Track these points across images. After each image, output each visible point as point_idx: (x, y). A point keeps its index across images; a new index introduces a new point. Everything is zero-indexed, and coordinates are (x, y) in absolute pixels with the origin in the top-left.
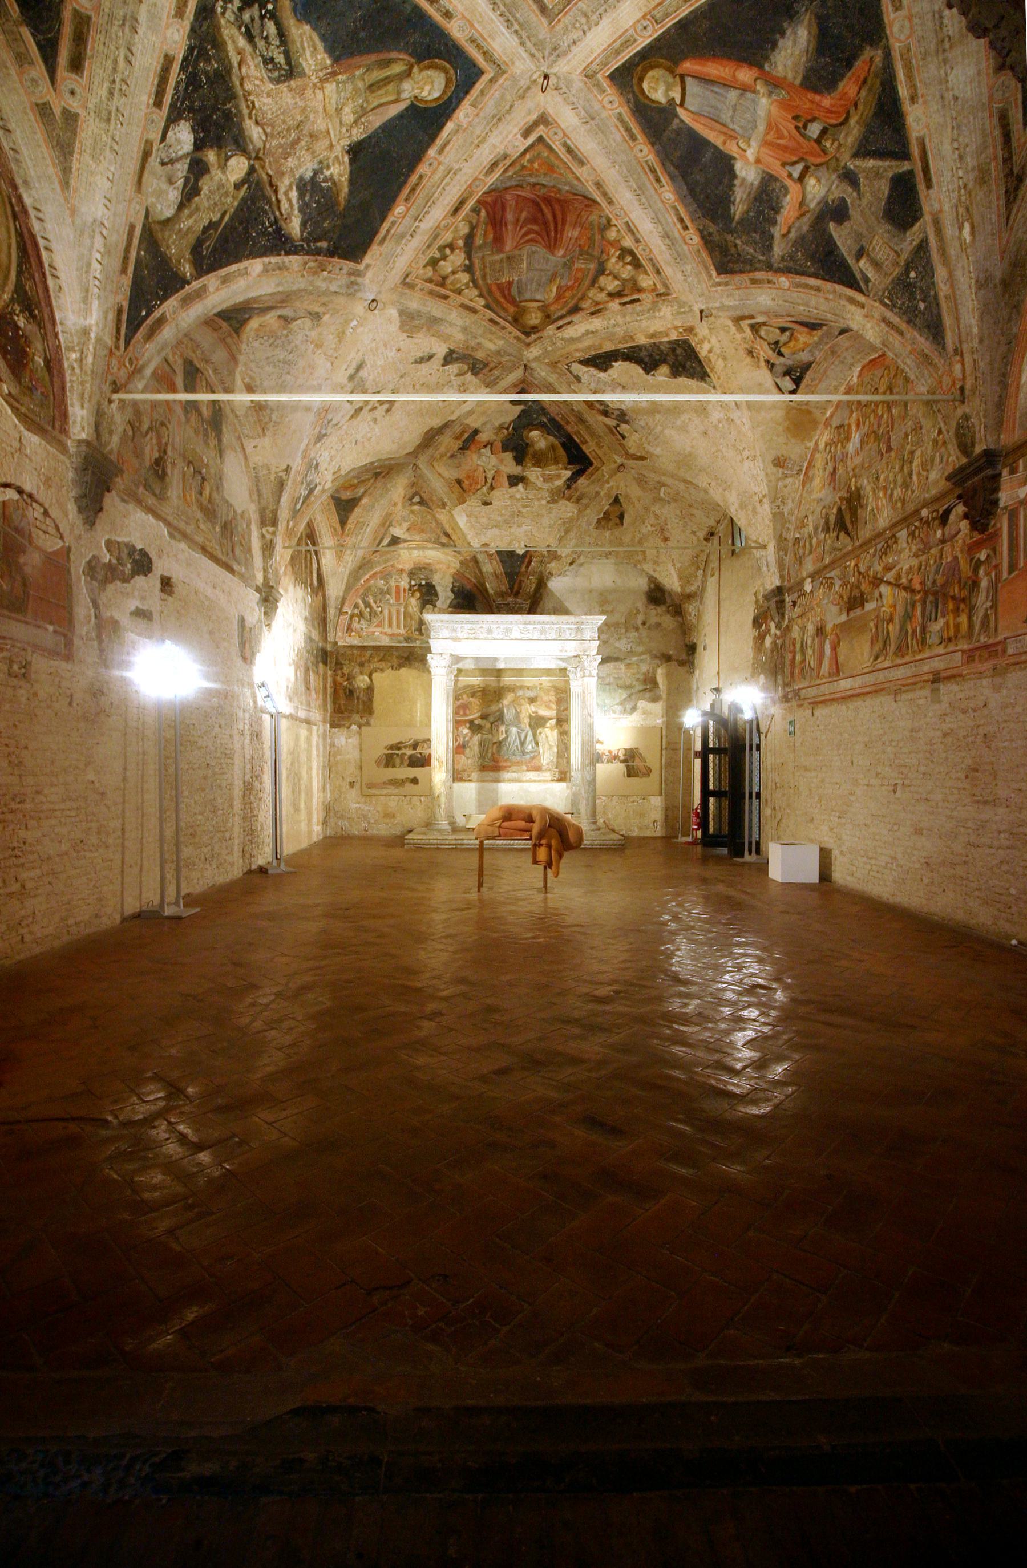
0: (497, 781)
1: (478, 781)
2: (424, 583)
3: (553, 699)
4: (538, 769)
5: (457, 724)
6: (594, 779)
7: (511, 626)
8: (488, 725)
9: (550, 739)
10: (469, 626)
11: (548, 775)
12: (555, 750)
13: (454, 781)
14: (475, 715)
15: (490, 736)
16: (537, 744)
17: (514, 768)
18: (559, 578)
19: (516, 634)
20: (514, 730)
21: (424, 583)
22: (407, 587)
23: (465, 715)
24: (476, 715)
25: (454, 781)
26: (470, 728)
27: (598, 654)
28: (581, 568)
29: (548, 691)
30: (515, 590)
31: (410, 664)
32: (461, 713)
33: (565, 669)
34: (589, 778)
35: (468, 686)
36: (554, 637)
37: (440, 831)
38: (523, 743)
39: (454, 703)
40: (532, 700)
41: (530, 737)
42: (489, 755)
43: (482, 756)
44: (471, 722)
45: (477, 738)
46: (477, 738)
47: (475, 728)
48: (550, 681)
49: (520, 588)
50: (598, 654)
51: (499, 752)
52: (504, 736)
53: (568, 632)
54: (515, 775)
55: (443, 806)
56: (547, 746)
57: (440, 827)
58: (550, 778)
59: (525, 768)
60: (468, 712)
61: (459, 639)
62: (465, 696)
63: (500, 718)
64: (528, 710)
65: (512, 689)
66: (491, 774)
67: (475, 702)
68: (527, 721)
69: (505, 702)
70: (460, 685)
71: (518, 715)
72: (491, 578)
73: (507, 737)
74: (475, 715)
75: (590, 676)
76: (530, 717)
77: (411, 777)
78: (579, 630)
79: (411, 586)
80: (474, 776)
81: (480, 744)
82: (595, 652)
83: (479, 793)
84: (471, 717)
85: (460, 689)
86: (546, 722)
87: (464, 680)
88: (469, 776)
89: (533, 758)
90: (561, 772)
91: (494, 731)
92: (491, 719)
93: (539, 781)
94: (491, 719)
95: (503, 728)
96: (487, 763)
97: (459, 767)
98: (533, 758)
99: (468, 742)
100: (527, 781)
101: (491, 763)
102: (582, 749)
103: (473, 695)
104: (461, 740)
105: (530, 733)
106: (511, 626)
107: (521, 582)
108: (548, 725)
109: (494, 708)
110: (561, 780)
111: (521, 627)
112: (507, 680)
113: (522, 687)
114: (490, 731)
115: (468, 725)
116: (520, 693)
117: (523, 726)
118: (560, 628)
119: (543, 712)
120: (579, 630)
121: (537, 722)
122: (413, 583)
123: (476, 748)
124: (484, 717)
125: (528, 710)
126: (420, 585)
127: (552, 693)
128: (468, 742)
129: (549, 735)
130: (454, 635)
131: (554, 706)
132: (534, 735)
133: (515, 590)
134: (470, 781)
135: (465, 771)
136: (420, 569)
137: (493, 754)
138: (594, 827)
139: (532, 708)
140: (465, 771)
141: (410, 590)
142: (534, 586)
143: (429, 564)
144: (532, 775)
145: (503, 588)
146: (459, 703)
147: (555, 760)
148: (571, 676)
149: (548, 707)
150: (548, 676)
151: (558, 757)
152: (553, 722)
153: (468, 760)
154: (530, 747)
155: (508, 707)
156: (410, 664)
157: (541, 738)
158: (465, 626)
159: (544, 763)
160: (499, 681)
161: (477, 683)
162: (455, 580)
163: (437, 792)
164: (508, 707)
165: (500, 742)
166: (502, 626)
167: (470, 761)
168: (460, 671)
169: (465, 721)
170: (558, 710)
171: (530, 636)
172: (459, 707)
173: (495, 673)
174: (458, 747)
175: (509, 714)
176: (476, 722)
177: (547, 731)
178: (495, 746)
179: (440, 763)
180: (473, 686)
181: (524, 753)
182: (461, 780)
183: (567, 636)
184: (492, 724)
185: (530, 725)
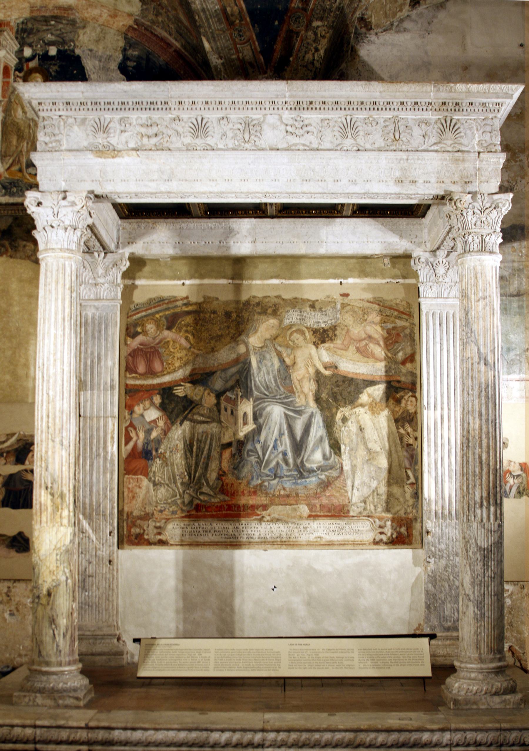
0: (234, 543)
1: (182, 544)
2: (53, 51)
3: (377, 331)
4: (339, 512)
5: (131, 396)
6: (499, 544)
7: (256, 115)
8: (210, 400)
9: (371, 434)
10: (144, 116)
11: (365, 530)
12: (383, 462)
13: (120, 544)
14: (174, 373)
15: (213, 428)
16: (336, 447)
17: (276, 510)
18: (387, 37)
19: (271, 135)
20: (276, 412)
21: (53, 51)
22: (13, 62)
23: (151, 373)
24: (179, 374)
25: (120, 544)
26: (163, 407)
27: (503, 189)
28: (441, 15)
29: (365, 312)
30: (277, 55)
31: (15, 248)
32: (142, 368)
33: (408, 257)
34: (484, 541)
35: (161, 301)
36: (380, 143)
37: (53, 694)
38: (299, 447)
39: (123, 343)
40: (323, 336)
41: (318, 430)
42: (213, 476)
43: (194, 479)
44: (166, 392)
45: (179, 433)
46: (179, 433)
47: (176, 408)
48: (369, 288)
49: (289, 49)
50: (503, 189)
51: (236, 468)
52: (251, 426)
53: (417, 132)
54: (278, 529)
55: (63, 622)
56: (362, 452)
57: (53, 682)
58: (369, 536)
59: (304, 510)
60: (157, 366)
61: (113, 152)
62: (151, 327)
63: (240, 381)
64: (311, 359)
65: (272, 308)
66: (217, 525)
67: (177, 341)
68: (309, 388)
69: (254, 340)
70: (139, 298)
71: (285, 371)
72: (215, 26)
73: (259, 430)
74: (174, 373)
75: (483, 249)
76: (319, 378)
77: (12, 532)
78: (448, 126)
79: (22, 61)
80: (173, 530)
81: (189, 447)
82: (495, 184)
83: (185, 576)
84: (167, 379)
85: (137, 310)
86: (359, 391)
87: (148, 286)
88: (160, 530)
89: (326, 485)
90: (398, 521)
91: (225, 416)
92: (218, 384)
93: (343, 544)
94: (218, 384)
95: (247, 407)
96: (208, 496)
97: (135, 507)
98: (326, 485)
99: (158, 442)
100: (310, 545)
101: (218, 500)
102: (464, 457)
103: (171, 323)
104: (139, 438)
105: (318, 420)
106: (256, 115)
107: (291, 35)
108: (364, 398)
109: (224, 355)
110: (399, 540)
111: (287, 115)
112: (260, 286)
113: (295, 303)
114: (215, 415)
115: (157, 399)
116: (292, 317)
117: (299, 401)
118: (396, 121)
119: (352, 366)
120: (448, 126)
121: (337, 391)
122: (28, 52)
123: (178, 459)
124: (199, 378)
125: (311, 359)
126: (45, 57)
127: (374, 317)
128: (158, 442)
129: (368, 423)
130: (101, 139)
131: (379, 351)
132: (329, 425)
133: (277, 55)
134: (162, 543)
135: (147, 517)
136: (46, 20)
137: (221, 475)
138: (499, 683)
139: (324, 355)
140: (147, 517)
141: (19, 68)
142: (323, 45)
143: (69, 8)
144: (322, 529)
145: (247, 52)
146: (135, 343)
147: (383, 489)
148: (423, 272)
149: (364, 353)
150: (363, 274)
151: (389, 484)
152: (378, 391)
153: (158, 491)
154: (318, 456)
155: (261, 352)
156: (15, 248)
157: (347, 433)
158: (134, 116)
159: (356, 497)
160: (238, 288)
161: (182, 293)
162: (129, 44)
163: (46, 581)
164: (261, 352)
165: (241, 444)
166: (234, 116)
167: (162, 491)
168: (137, 264)
169: (149, 391)
170: (390, 361)
171: (311, 139)
172: (134, 354)
173: (229, 270)
174: (133, 455)
175: (263, 373)
176: (180, 392)
177: (362, 415)
178: (227, 454)
179: (57, 497)
180: (173, 300)
181: (302, 471)
182: (139, 540)
183: (417, 141)
184: (219, 395)
185: (318, 399)
